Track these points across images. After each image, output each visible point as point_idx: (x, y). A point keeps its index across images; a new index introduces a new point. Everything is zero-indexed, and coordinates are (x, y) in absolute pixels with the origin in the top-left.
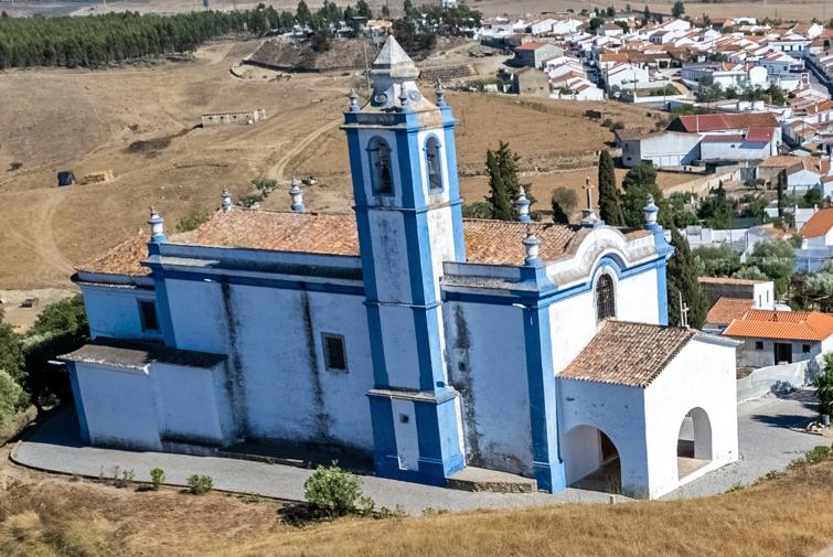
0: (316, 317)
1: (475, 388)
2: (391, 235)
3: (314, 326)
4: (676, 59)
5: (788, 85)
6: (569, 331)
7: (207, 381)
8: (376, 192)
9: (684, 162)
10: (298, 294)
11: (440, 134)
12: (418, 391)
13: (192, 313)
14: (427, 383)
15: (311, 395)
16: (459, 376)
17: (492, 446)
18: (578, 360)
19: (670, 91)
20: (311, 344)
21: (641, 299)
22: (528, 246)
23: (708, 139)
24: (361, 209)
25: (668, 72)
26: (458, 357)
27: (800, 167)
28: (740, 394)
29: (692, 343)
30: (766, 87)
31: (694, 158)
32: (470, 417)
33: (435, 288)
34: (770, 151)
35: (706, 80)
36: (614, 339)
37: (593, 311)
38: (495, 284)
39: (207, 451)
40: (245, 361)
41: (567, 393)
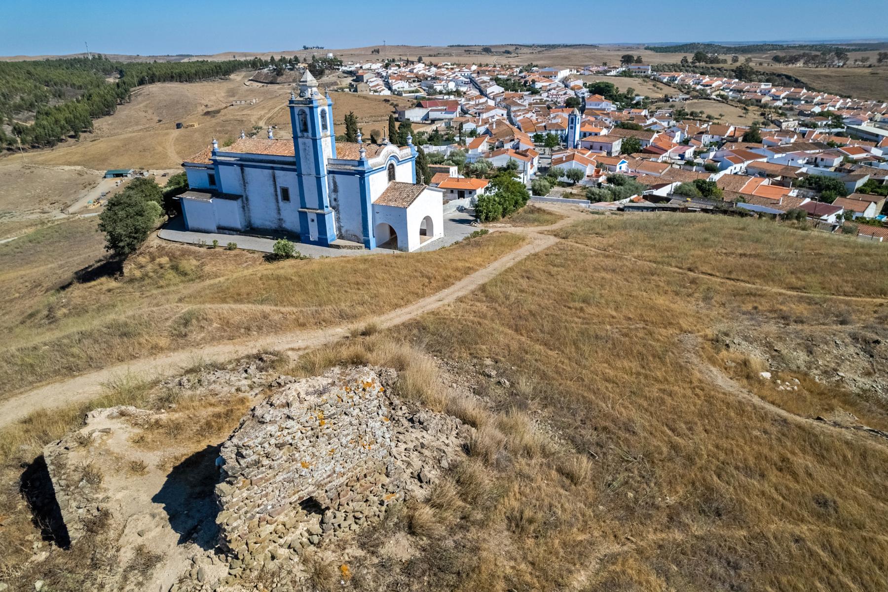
0: (278, 180)
1: (340, 208)
4: (419, 79)
5: (463, 89)
6: (377, 185)
7: (235, 205)
8: (301, 131)
9: (422, 119)
10: (271, 171)
11: (326, 108)
13: (229, 179)
14: (321, 206)
15: (276, 211)
16: (334, 203)
17: (347, 231)
18: (380, 197)
19: (417, 91)
20: (276, 191)
21: (406, 173)
22: (361, 152)
23: (432, 110)
24: (295, 138)
25: (416, 84)
26: (333, 196)
27: (468, 121)
28: (444, 211)
29: (425, 190)
30: (454, 90)
31: (426, 117)
32: (338, 220)
33: (324, 168)
34: (456, 115)
35: (431, 87)
36: (395, 189)
37: (386, 178)
38: (348, 167)
40: (250, 198)
41: (376, 210)
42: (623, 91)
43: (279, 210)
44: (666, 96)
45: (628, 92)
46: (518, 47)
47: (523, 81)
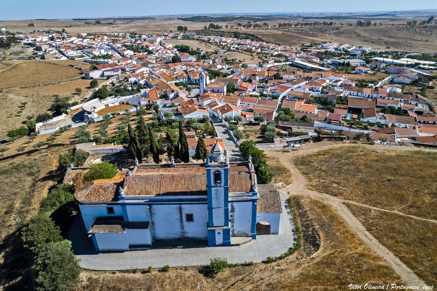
2: (219, 193)
3: (183, 212)
5: (110, 53)
9: (100, 77)
10: (178, 206)
12: (223, 226)
25: (79, 51)
31: (102, 75)
39: (147, 248)
42: (195, 49)
43: (183, 227)
44: (216, 51)
45: (197, 49)
46: (115, 19)
47: (140, 46)
